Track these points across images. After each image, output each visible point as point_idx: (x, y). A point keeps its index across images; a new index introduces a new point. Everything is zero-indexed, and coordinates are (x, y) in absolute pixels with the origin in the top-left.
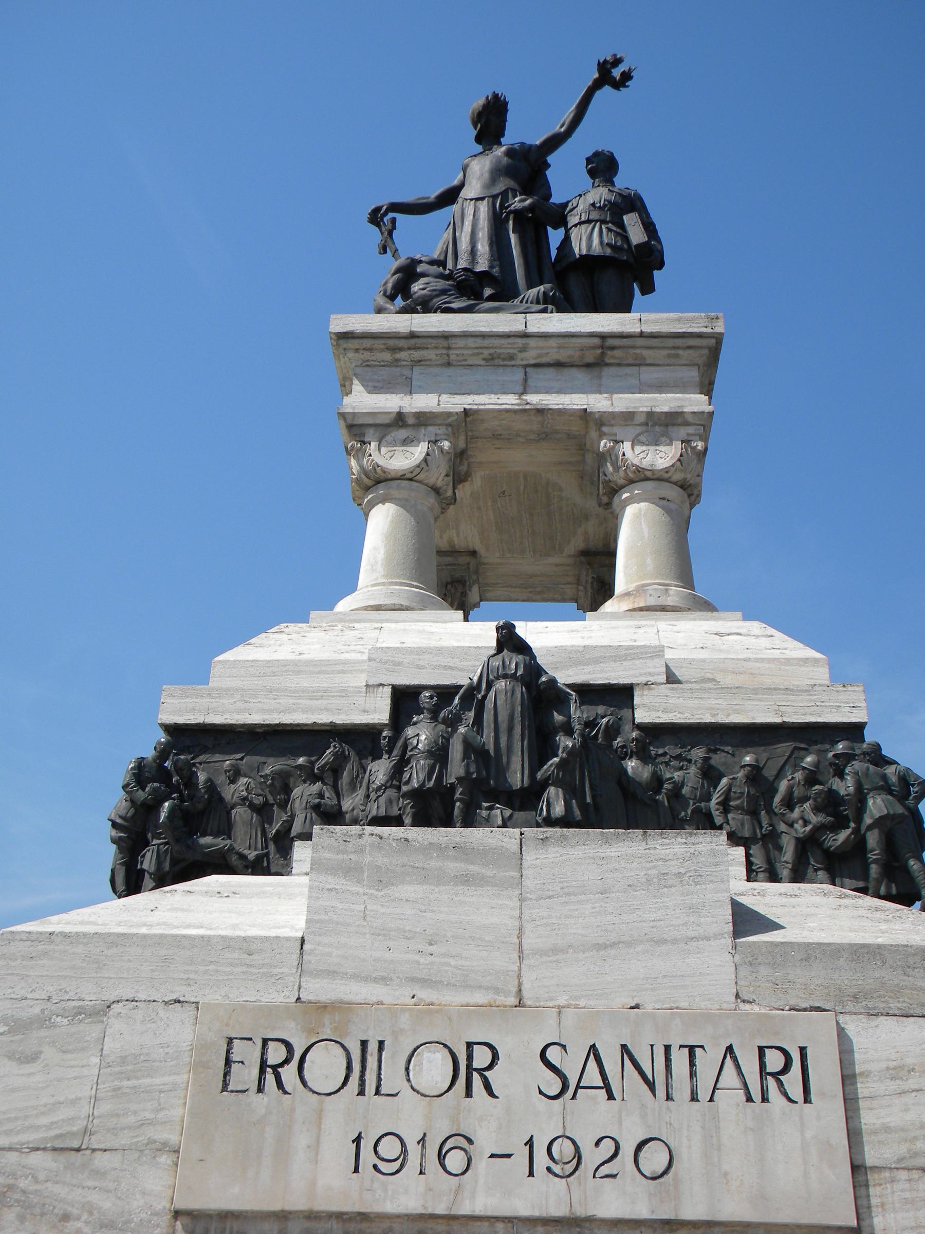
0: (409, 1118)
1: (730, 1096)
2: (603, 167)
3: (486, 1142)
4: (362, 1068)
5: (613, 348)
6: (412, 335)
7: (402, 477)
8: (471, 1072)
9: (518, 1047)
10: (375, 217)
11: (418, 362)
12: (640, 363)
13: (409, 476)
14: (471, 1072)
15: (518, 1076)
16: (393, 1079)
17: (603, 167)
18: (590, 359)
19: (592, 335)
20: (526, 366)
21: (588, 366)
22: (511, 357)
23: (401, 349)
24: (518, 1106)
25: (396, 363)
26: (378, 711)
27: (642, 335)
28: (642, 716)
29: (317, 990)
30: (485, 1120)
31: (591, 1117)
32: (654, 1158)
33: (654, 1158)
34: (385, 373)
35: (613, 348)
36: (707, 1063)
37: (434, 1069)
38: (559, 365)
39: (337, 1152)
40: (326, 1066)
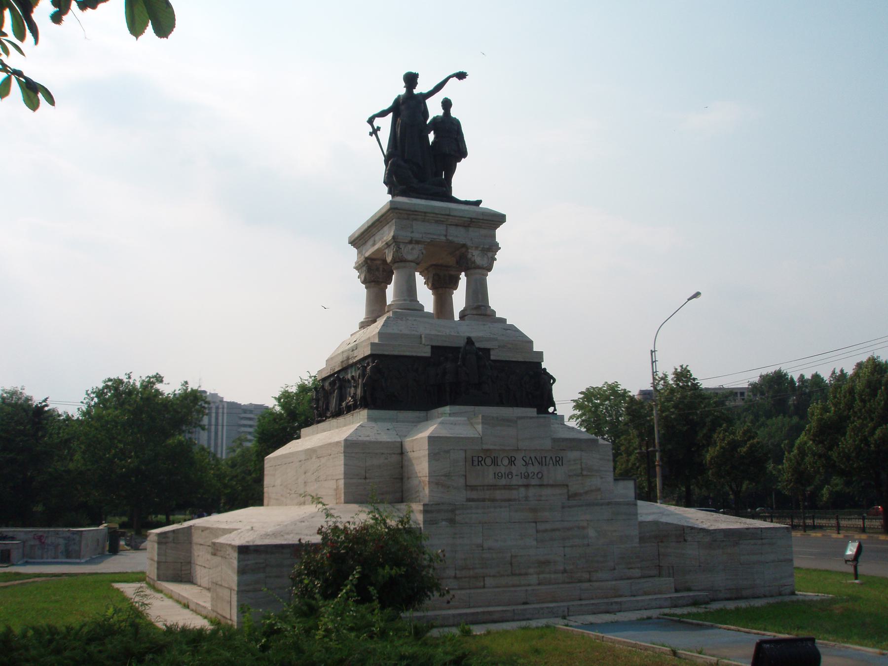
0: (503, 469)
1: (551, 465)
2: (447, 104)
3: (514, 473)
4: (495, 462)
7: (411, 261)
8: (512, 461)
9: (519, 456)
10: (371, 121)
11: (416, 219)
12: (480, 227)
14: (512, 461)
15: (519, 463)
16: (499, 463)
17: (447, 104)
24: (519, 467)
25: (408, 219)
26: (426, 352)
28: (492, 358)
29: (485, 447)
30: (514, 469)
31: (532, 469)
32: (540, 476)
33: (540, 476)
36: (548, 459)
37: (506, 462)
38: (457, 225)
39: (491, 476)
40: (488, 461)
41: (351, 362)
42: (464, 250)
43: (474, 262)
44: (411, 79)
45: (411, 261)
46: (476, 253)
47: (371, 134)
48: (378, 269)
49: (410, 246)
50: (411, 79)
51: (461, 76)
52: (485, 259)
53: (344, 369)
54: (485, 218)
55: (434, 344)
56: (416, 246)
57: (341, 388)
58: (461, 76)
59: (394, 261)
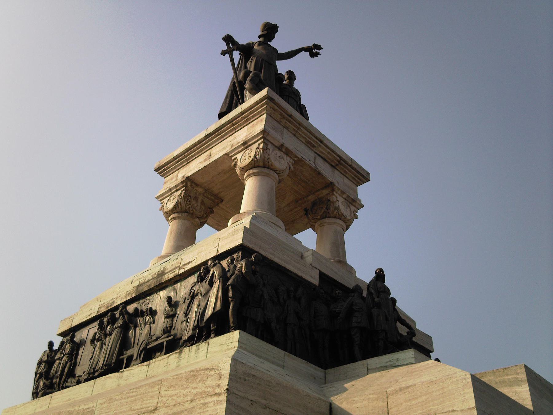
5: (341, 164)
6: (291, 116)
11: (287, 128)
13: (278, 172)
18: (333, 164)
19: (339, 156)
20: (316, 153)
21: (332, 165)
22: (314, 146)
23: (284, 118)
25: (279, 122)
27: (350, 166)
34: (276, 123)
35: (341, 164)
38: (324, 159)
41: (166, 278)
42: (325, 192)
43: (337, 208)
44: (270, 31)
45: (275, 171)
46: (341, 199)
47: (223, 53)
48: (196, 199)
49: (279, 153)
50: (270, 31)
51: (313, 51)
52: (348, 210)
53: (143, 295)
54: (353, 165)
55: (324, 271)
56: (285, 157)
57: (125, 328)
58: (313, 51)
59: (253, 165)
